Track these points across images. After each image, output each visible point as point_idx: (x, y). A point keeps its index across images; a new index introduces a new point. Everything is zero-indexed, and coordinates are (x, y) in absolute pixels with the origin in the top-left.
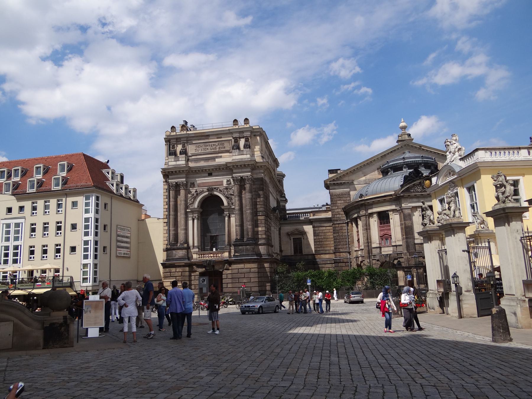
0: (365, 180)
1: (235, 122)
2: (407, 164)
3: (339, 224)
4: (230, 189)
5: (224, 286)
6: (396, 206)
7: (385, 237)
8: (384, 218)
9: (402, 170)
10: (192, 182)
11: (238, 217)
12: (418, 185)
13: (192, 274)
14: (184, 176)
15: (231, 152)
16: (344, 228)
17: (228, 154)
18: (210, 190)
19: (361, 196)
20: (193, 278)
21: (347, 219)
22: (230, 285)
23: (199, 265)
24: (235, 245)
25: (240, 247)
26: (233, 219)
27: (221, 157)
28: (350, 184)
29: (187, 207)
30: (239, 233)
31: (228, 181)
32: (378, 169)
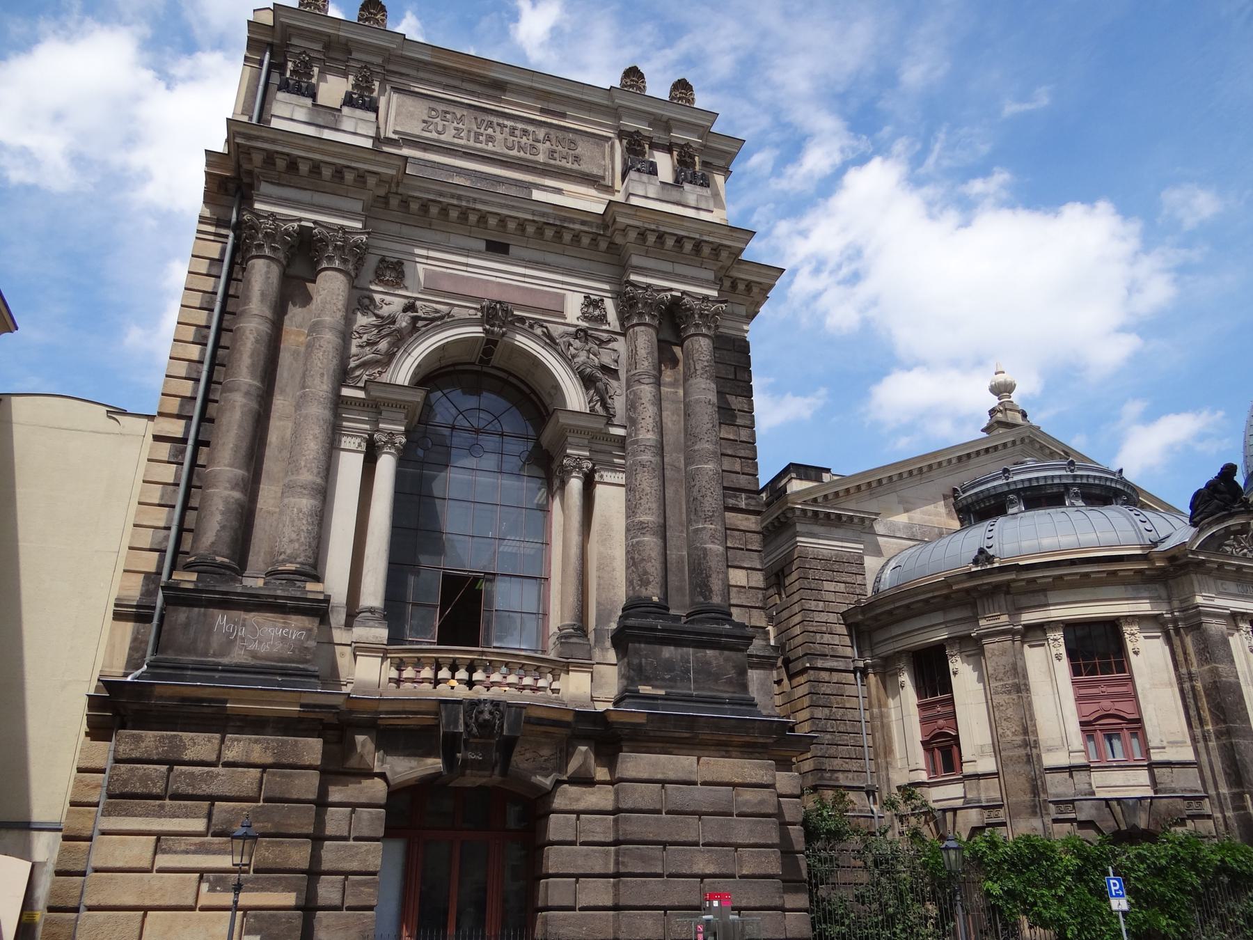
0: (909, 527)
2: (1080, 486)
3: (831, 670)
4: (602, 343)
6: (1153, 599)
7: (1114, 725)
8: (1096, 650)
9: (1062, 504)
10: (392, 256)
12: (1236, 533)
13: (336, 794)
14: (358, 207)
16: (850, 690)
17: (593, 192)
19: (983, 556)
20: (336, 820)
21: (861, 655)
23: (400, 729)
25: (668, 652)
27: (559, 191)
28: (862, 526)
29: (343, 375)
31: (590, 302)
32: (945, 497)
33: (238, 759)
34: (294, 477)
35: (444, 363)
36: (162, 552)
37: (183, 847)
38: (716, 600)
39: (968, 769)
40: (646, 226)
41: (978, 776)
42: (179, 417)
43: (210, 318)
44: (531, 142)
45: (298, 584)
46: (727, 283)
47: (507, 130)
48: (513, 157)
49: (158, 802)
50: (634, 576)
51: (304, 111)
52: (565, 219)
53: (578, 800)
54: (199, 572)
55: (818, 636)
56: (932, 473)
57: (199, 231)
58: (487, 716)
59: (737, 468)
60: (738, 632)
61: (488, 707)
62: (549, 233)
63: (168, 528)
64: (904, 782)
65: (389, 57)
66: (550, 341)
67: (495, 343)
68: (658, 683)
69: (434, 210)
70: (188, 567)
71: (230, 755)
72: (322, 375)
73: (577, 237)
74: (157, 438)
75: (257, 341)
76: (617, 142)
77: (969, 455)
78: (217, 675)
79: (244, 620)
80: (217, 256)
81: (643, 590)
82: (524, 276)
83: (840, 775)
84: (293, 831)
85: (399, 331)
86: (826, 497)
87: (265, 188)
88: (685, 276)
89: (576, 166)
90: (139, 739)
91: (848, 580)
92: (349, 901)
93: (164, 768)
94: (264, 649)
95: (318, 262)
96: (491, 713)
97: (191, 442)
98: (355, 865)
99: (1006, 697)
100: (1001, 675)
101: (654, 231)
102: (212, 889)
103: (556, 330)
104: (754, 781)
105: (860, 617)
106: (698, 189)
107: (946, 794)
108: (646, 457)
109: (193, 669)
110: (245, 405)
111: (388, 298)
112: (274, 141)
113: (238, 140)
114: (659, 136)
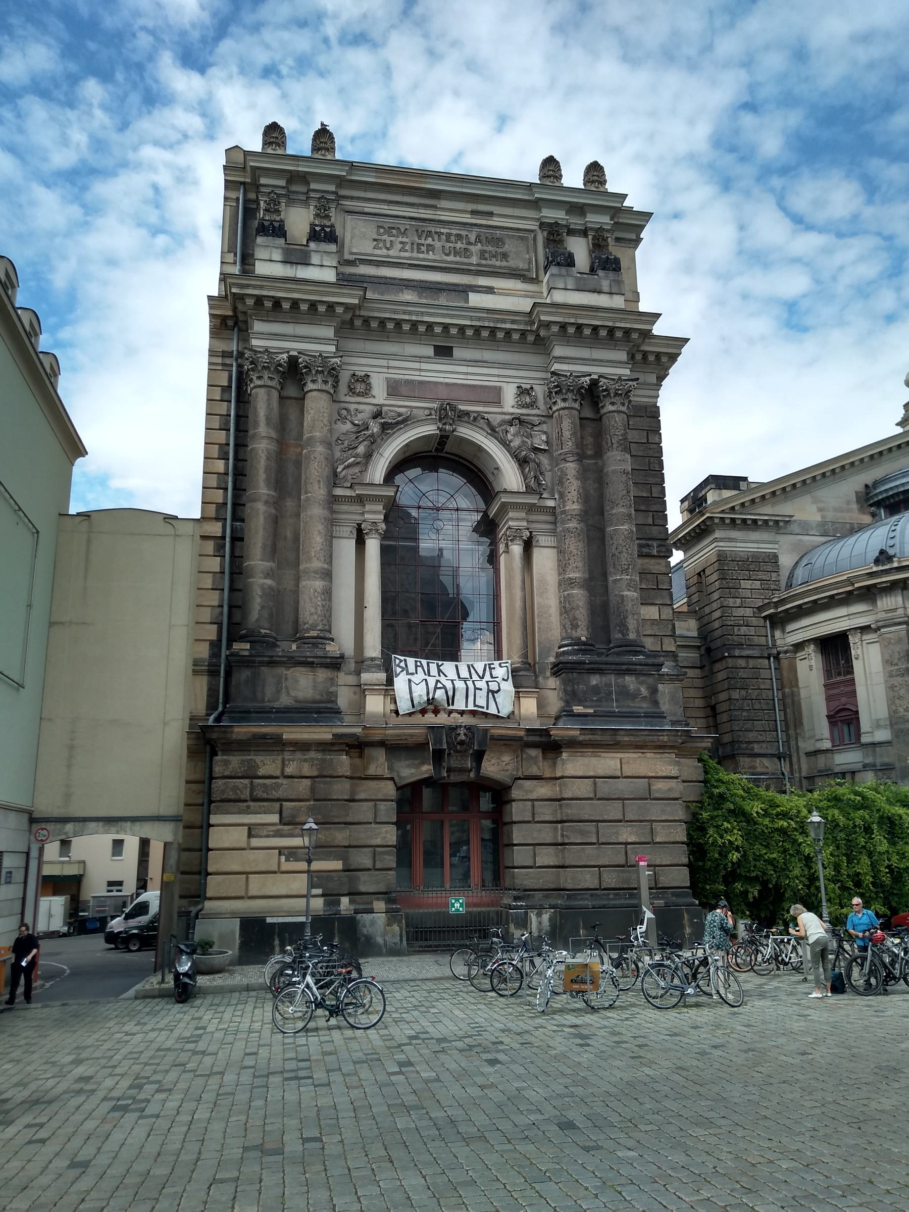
1: (551, 166)
5: (520, 856)
10: (360, 371)
11: (575, 546)
14: (329, 332)
15: (536, 281)
18: (448, 413)
19: (883, 557)
22: (546, 857)
24: (558, 669)
25: (595, 680)
26: (545, 560)
27: (490, 290)
29: (334, 479)
30: (582, 614)
31: (522, 392)
33: (294, 774)
34: (308, 565)
35: (407, 454)
36: (220, 625)
37: (265, 833)
38: (632, 636)
39: (865, 739)
40: (567, 320)
41: (873, 744)
42: (217, 519)
43: (228, 436)
44: (464, 246)
45: (320, 646)
46: (639, 357)
47: (444, 237)
48: (451, 262)
49: (246, 804)
50: (567, 621)
51: (280, 251)
52: (498, 320)
53: (532, 792)
54: (251, 642)
55: (736, 628)
56: (846, 473)
57: (210, 364)
58: (463, 737)
59: (650, 521)
60: (650, 661)
61: (462, 731)
62: (485, 334)
63: (221, 606)
64: (812, 749)
65: (341, 182)
66: (492, 431)
67: (447, 437)
68: (587, 704)
69: (390, 326)
70: (242, 639)
71: (289, 770)
72: (319, 481)
73: (508, 333)
74: (204, 537)
75: (268, 459)
76: (539, 231)
77: (881, 453)
78: (273, 716)
79: (286, 674)
80: (226, 384)
81: (574, 632)
82: (467, 374)
83: (756, 746)
84: (336, 820)
85: (372, 435)
86: (743, 504)
87: (258, 326)
88: (601, 361)
89: (504, 264)
90: (226, 763)
91: (764, 577)
92: (378, 866)
93: (246, 781)
94: (301, 695)
95: (304, 384)
96: (465, 734)
97: (228, 539)
98: (378, 841)
99: (899, 679)
100: (896, 661)
101: (573, 324)
102: (287, 860)
103: (496, 420)
104: (664, 774)
105: (772, 611)
106: (611, 274)
107: (847, 758)
108: (573, 524)
109: (256, 712)
110: (265, 512)
111: (361, 407)
112: (261, 287)
113: (234, 290)
114: (576, 222)
